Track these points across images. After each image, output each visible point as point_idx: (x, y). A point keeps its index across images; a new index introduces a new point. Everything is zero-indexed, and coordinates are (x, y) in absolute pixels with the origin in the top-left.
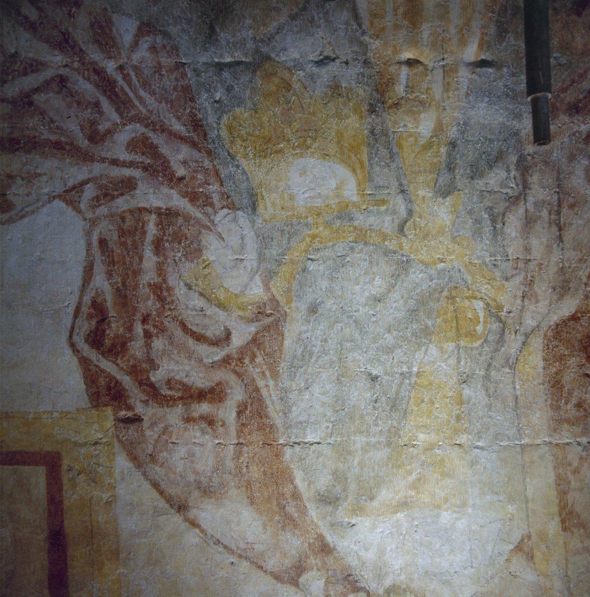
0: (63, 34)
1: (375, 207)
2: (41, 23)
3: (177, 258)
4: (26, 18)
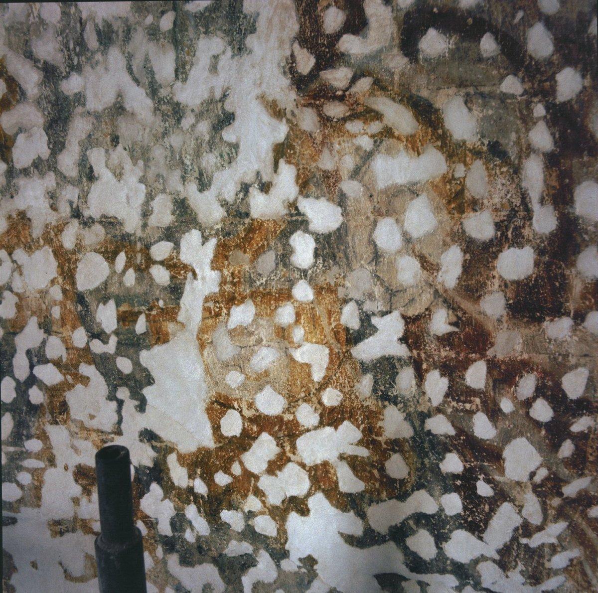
1: (136, 309)
3: (522, 214)
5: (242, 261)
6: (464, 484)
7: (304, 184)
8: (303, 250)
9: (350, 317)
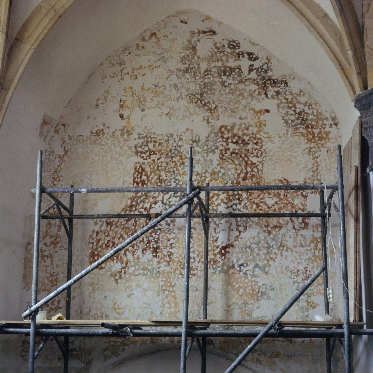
5: (213, 176)
6: (239, 199)
7: (221, 168)
8: (220, 174)
9: (226, 182)
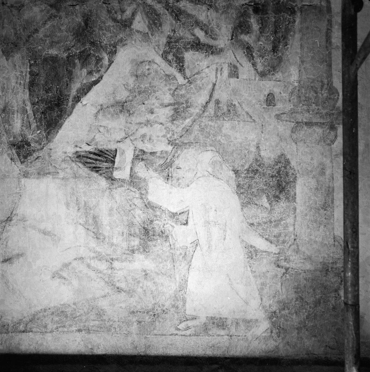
0: (178, 20)
2: (192, 26)
4: (202, 29)
